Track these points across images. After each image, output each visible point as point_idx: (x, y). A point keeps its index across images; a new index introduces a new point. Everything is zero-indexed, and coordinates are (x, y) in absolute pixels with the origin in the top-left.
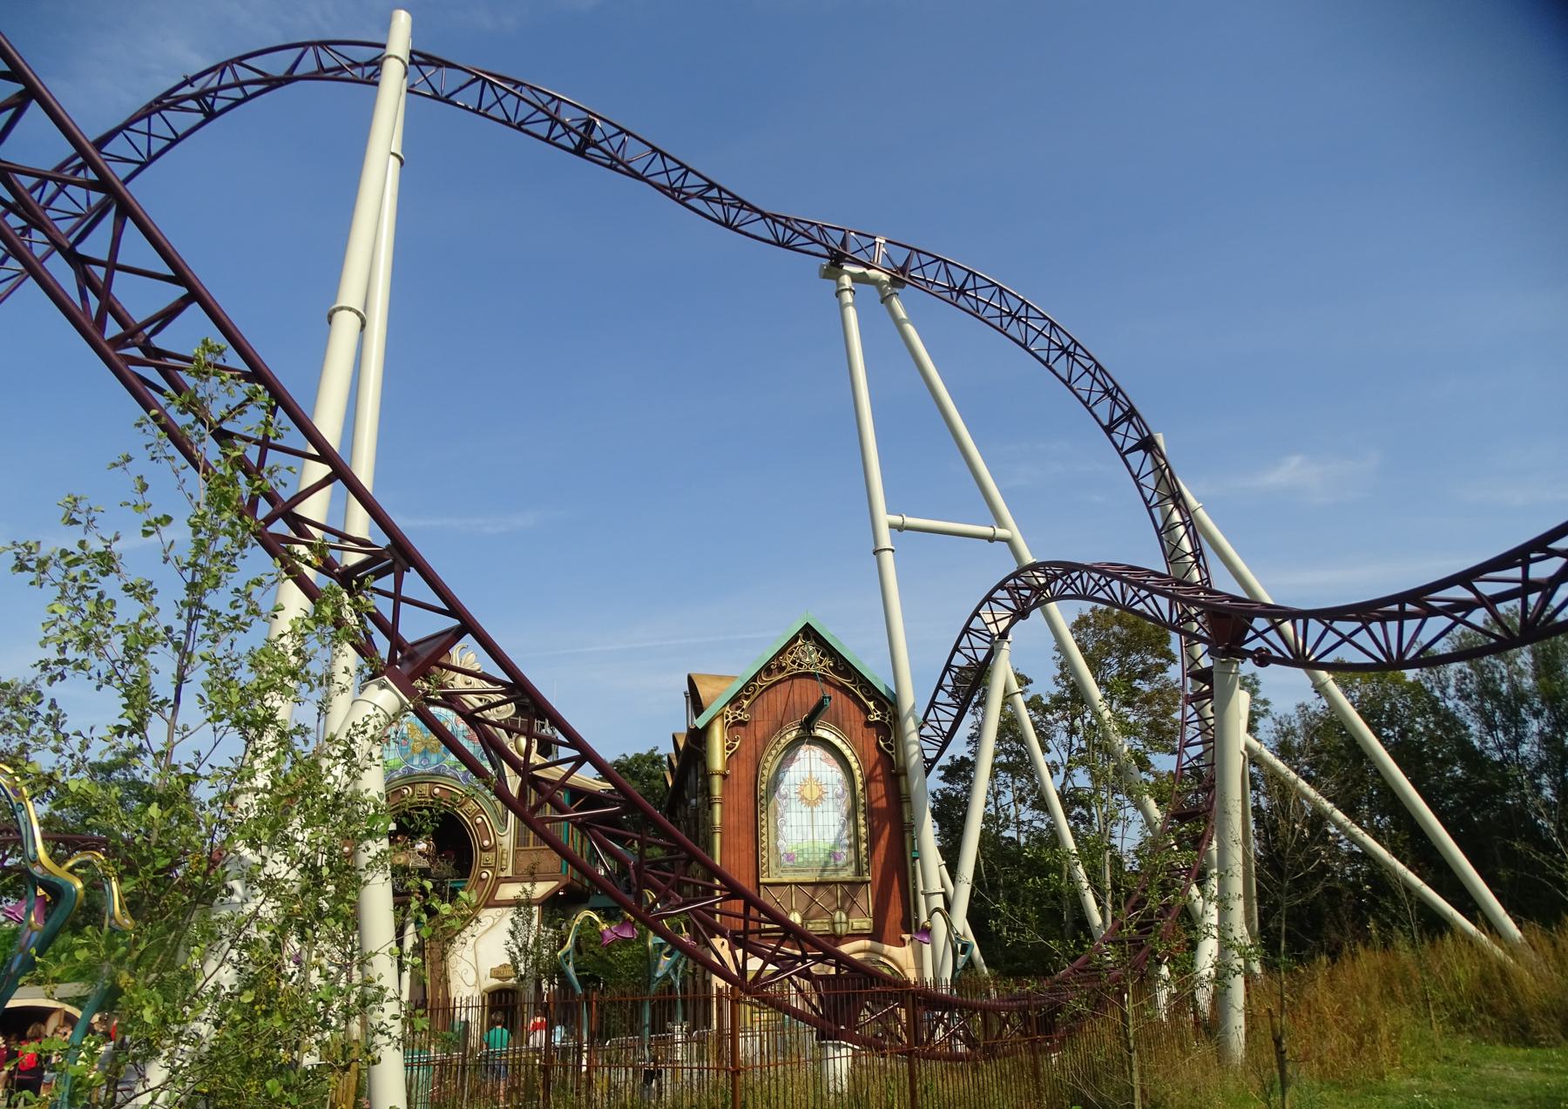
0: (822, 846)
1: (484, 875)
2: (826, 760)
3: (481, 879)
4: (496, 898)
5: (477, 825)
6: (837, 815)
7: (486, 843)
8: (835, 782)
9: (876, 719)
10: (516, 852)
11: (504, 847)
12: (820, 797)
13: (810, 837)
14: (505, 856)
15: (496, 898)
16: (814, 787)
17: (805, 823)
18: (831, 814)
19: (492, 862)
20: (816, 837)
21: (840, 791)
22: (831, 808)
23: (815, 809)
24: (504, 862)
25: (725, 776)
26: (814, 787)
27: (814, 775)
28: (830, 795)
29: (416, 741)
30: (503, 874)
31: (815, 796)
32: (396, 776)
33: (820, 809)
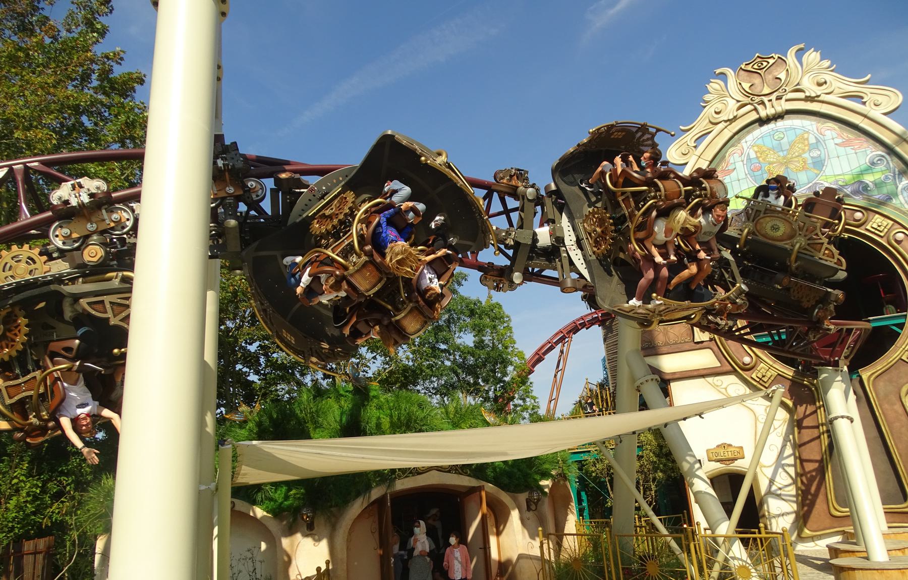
5: (899, 242)
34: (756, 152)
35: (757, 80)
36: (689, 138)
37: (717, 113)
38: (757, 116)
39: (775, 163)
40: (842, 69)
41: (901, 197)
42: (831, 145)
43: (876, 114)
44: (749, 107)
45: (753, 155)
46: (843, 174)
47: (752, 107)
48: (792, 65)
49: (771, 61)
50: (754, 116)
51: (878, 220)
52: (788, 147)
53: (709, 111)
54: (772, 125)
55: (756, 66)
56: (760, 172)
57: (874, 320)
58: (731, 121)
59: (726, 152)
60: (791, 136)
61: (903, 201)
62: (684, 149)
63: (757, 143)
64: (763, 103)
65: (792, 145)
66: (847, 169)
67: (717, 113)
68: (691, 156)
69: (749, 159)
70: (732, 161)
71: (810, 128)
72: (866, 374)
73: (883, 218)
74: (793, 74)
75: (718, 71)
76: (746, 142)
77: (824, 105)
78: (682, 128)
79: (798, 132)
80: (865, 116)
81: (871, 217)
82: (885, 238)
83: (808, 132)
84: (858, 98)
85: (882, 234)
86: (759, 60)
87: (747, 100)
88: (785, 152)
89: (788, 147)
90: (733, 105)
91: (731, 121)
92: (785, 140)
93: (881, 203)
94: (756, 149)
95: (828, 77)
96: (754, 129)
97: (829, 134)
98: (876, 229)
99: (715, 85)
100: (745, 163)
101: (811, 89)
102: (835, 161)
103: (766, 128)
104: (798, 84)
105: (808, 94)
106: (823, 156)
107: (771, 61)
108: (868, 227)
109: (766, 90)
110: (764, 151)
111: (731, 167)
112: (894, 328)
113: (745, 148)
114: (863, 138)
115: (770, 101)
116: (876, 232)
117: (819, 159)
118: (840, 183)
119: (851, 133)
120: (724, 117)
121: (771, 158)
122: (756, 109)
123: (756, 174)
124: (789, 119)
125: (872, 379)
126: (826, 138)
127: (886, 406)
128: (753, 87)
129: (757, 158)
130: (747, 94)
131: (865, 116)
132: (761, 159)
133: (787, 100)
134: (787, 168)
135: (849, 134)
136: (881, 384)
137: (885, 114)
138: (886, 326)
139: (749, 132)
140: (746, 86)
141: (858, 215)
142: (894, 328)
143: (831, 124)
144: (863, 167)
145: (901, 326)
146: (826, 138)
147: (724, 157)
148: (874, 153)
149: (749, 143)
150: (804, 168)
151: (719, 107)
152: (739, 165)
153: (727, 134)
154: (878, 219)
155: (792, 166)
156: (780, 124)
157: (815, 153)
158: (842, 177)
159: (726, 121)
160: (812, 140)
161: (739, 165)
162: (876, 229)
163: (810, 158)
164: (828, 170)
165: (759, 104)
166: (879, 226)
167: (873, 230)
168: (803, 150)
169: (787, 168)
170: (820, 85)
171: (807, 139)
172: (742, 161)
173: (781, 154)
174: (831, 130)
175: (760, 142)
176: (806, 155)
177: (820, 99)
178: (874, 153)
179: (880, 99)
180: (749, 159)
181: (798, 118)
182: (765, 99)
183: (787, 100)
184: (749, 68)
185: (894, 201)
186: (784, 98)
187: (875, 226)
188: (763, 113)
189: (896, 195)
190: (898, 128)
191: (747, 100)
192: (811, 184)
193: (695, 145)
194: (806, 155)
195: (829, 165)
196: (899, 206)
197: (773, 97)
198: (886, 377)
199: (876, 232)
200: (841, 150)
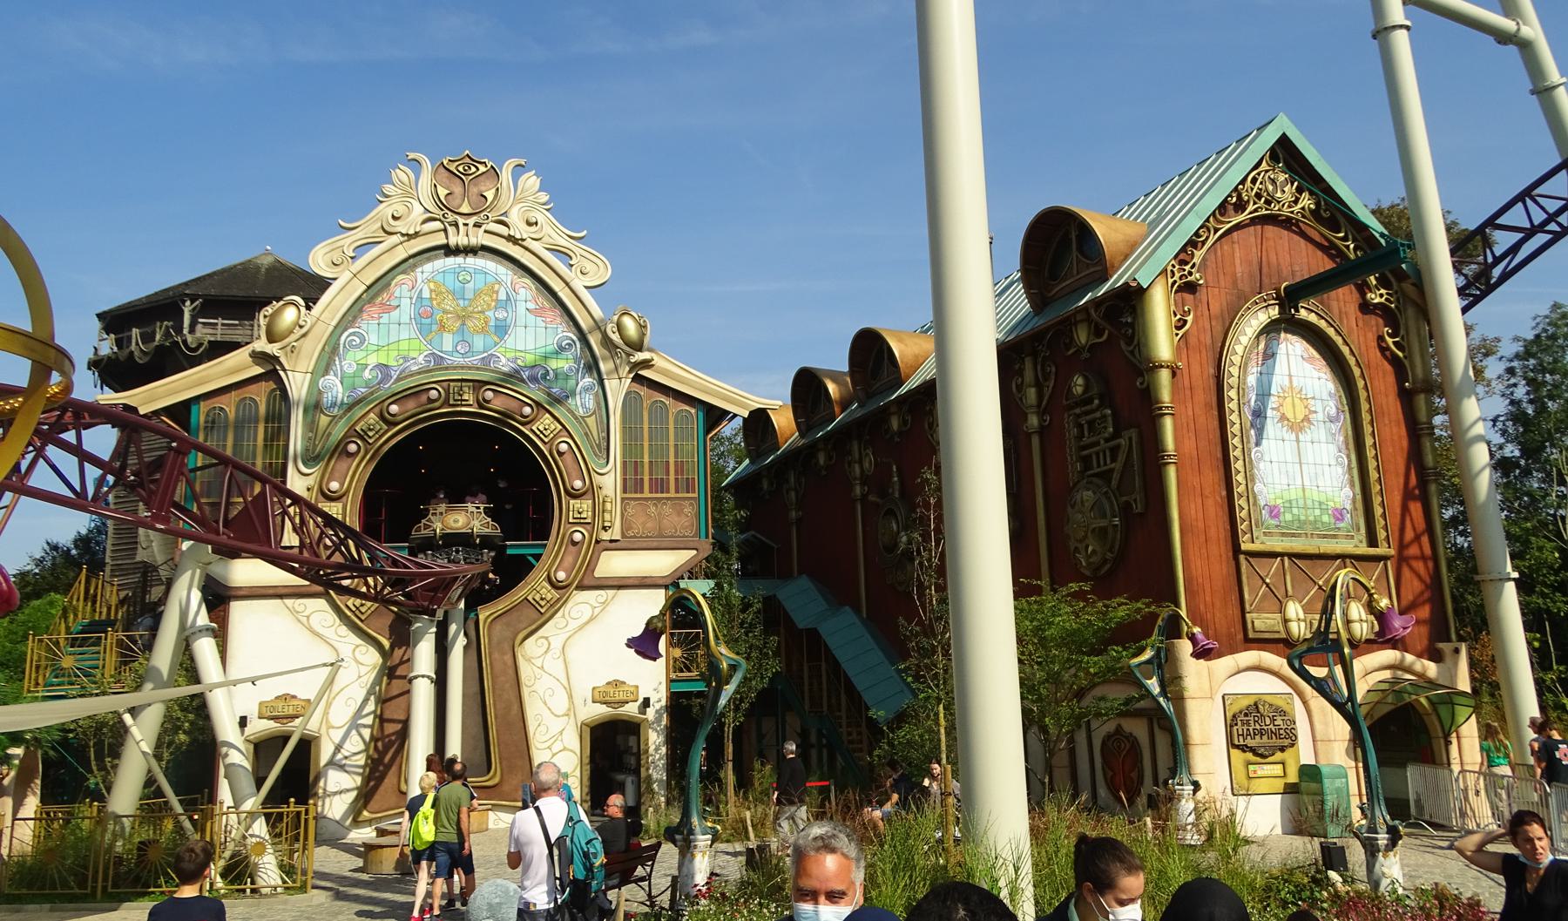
0: (1316, 498)
1: (577, 536)
2: (1310, 360)
3: (574, 543)
4: (597, 574)
5: (561, 454)
6: (1333, 449)
7: (578, 484)
8: (1325, 396)
11: (604, 492)
12: (1306, 419)
13: (1299, 482)
14: (608, 506)
15: (597, 574)
16: (1297, 401)
17: (1289, 459)
18: (1324, 446)
19: (587, 515)
21: (1333, 411)
22: (1323, 438)
23: (1301, 437)
24: (607, 517)
26: (1297, 401)
27: (1295, 384)
28: (1320, 416)
29: (445, 312)
30: (605, 536)
31: (1300, 417)
32: (414, 368)
33: (1309, 438)
34: (431, 291)
35: (458, 189)
36: (348, 242)
37: (394, 218)
38: (445, 241)
39: (451, 313)
40: (559, 211)
41: (578, 397)
42: (521, 308)
43: (579, 284)
44: (437, 225)
45: (426, 294)
46: (525, 352)
47: (442, 227)
48: (504, 184)
49: (482, 169)
50: (440, 240)
51: (547, 421)
52: (471, 296)
53: (385, 210)
54: (459, 260)
55: (461, 169)
56: (428, 321)
57: (511, 545)
58: (410, 237)
59: (392, 280)
60: (479, 282)
61: (579, 404)
62: (336, 257)
63: (436, 278)
64: (456, 225)
65: (478, 294)
66: (531, 346)
67: (394, 218)
68: (343, 271)
69: (420, 297)
70: (397, 294)
71: (504, 278)
72: (484, 614)
73: (552, 419)
74: (503, 197)
75: (412, 155)
76: (422, 273)
77: (527, 253)
79: (490, 279)
80: (567, 284)
81: (540, 416)
82: (548, 445)
83: (499, 283)
85: (546, 440)
86: (468, 160)
87: (438, 213)
88: (466, 302)
89: (471, 296)
90: (418, 212)
91: (410, 237)
92: (471, 285)
93: (557, 401)
94: (432, 285)
95: (541, 217)
96: (436, 257)
97: (522, 291)
98: (541, 432)
99: (402, 174)
100: (414, 302)
101: (520, 230)
102: (520, 330)
104: (505, 214)
105: (512, 233)
106: (508, 320)
107: (482, 169)
108: (534, 428)
109: (465, 209)
110: (441, 293)
111: (394, 303)
112: (530, 558)
113: (419, 281)
114: (558, 311)
115: (466, 225)
116: (541, 436)
117: (503, 324)
118: (519, 362)
119: (548, 300)
120: (401, 227)
121: (449, 304)
122: (445, 230)
123: (424, 321)
124: (483, 257)
125: (489, 620)
127: (496, 655)
128: (450, 197)
129: (431, 299)
130: (440, 204)
131: (567, 284)
132: (435, 302)
133: (486, 231)
135: (544, 302)
136: (498, 627)
137: (586, 287)
138: (523, 556)
139: (429, 260)
140: (442, 192)
141: (527, 410)
142: (530, 558)
143: (528, 281)
144: (550, 349)
145: (538, 557)
146: (519, 297)
147: (389, 284)
148: (565, 334)
149: (425, 275)
150: (483, 331)
151: (400, 209)
152: (405, 303)
153: (401, 254)
154: (547, 419)
155: (470, 324)
156: (470, 260)
157: (501, 314)
158: (523, 354)
159: (403, 235)
160: (503, 296)
161: (405, 303)
162: (541, 432)
163: (493, 318)
164: (510, 341)
165: (450, 225)
166: (545, 429)
167: (538, 433)
168: (489, 305)
170: (529, 224)
171: (497, 292)
172: (411, 298)
173: (461, 302)
174: (526, 291)
175: (439, 278)
176: (490, 314)
177: (524, 243)
178: (565, 334)
179: (589, 267)
180: (420, 297)
181: (493, 260)
182: (461, 221)
183: (486, 231)
184: (452, 168)
185: (570, 401)
186: (484, 227)
187: (541, 428)
188: (453, 241)
189: (573, 393)
190: (598, 312)
191: (438, 213)
192: (486, 354)
193: (353, 255)
194: (490, 314)
195: (513, 335)
196: (573, 408)
197: (471, 221)
198: (504, 619)
199: (541, 436)
200: (531, 318)
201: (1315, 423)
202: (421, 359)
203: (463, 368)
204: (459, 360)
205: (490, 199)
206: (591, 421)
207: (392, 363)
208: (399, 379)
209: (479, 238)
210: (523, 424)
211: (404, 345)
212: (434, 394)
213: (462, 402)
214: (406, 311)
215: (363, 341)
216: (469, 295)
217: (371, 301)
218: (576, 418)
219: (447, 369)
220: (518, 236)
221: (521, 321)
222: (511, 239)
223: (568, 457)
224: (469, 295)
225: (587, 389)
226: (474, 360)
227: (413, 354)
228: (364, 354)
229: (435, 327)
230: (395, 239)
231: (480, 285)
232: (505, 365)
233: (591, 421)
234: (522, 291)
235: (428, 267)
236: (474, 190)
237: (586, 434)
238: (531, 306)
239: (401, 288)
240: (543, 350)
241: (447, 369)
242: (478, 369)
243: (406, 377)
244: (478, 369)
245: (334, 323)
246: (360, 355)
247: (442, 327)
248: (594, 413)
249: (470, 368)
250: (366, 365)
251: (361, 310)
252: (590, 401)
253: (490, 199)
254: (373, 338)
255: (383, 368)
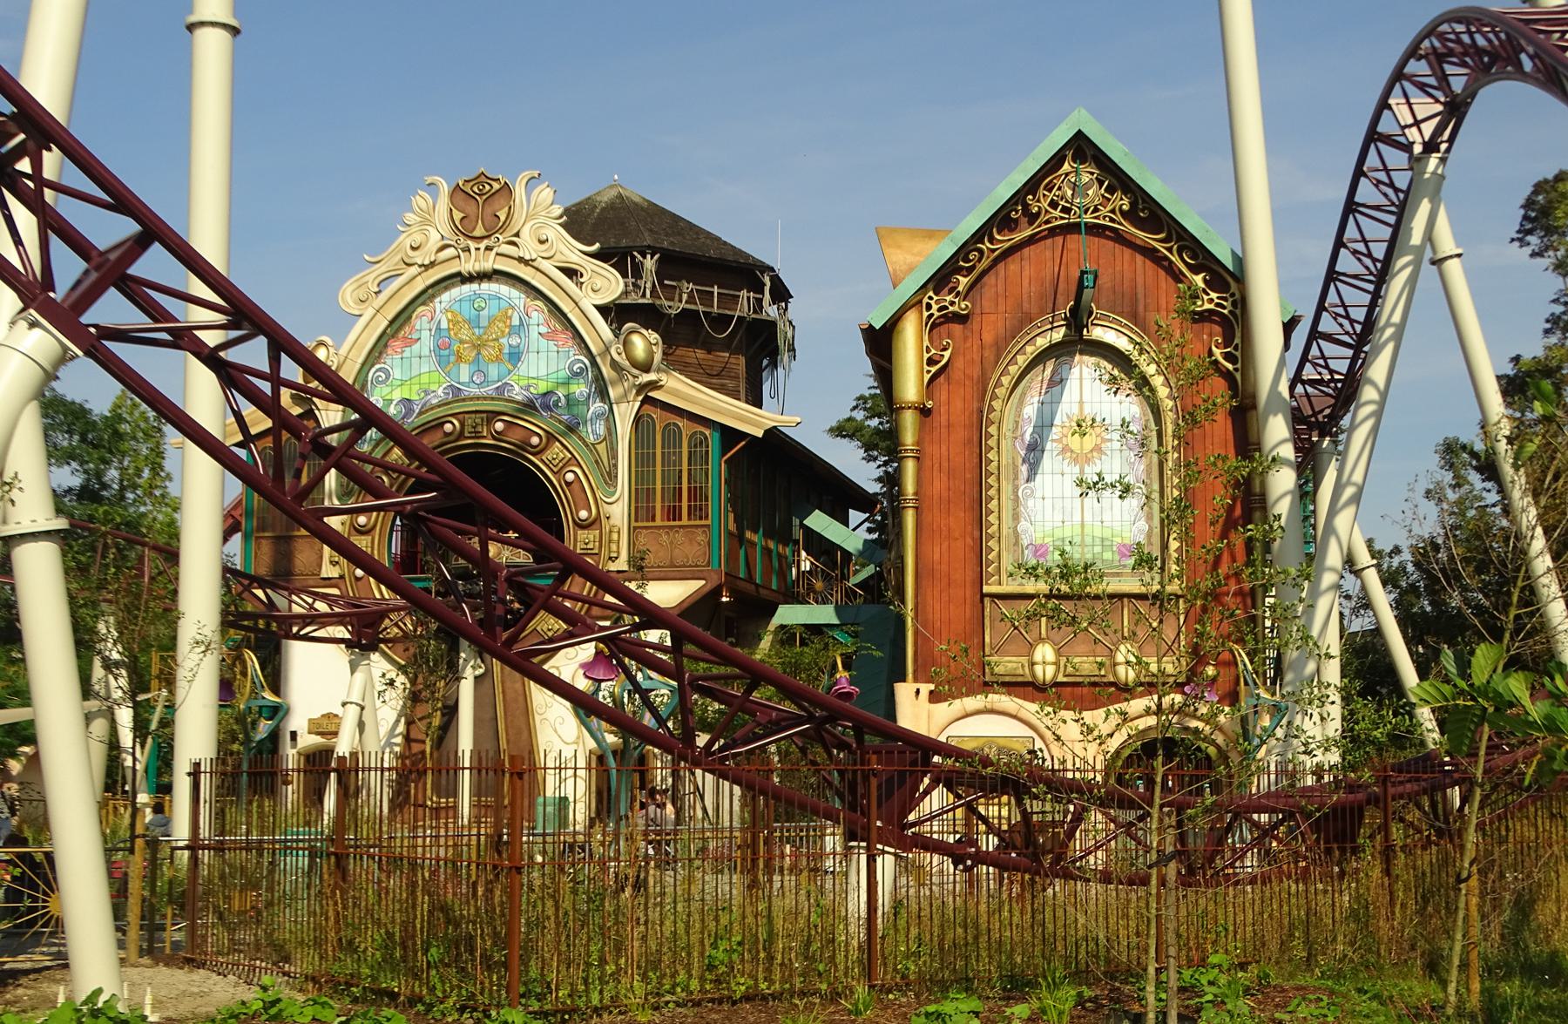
7: (583, 514)
9: (1207, 306)
10: (632, 531)
11: (612, 521)
13: (1077, 517)
20: (1088, 517)
25: (924, 412)
29: (462, 342)
32: (435, 401)
34: (449, 321)
36: (372, 276)
37: (413, 248)
42: (534, 334)
45: (444, 325)
46: (537, 378)
52: (486, 324)
53: (405, 241)
54: (475, 286)
55: (476, 189)
58: (427, 267)
60: (492, 309)
62: (362, 294)
65: (492, 320)
67: (413, 248)
69: (439, 328)
70: (417, 327)
71: (517, 302)
74: (516, 216)
75: (429, 180)
78: (367, 258)
84: (571, 273)
89: (486, 324)
90: (434, 239)
91: (427, 267)
96: (453, 285)
97: (535, 314)
99: (421, 200)
102: (533, 356)
103: (467, 288)
109: (479, 231)
110: (458, 322)
111: (415, 336)
115: (478, 249)
120: (419, 258)
124: (497, 281)
126: (531, 321)
128: (465, 221)
129: (449, 329)
130: (457, 230)
133: (497, 254)
134: (479, 353)
139: (447, 288)
140: (458, 215)
146: (531, 321)
147: (410, 317)
149: (443, 305)
150: (498, 359)
151: (417, 238)
152: (425, 334)
153: (419, 285)
155: (484, 352)
156: (485, 286)
157: (514, 341)
159: (420, 266)
160: (516, 322)
161: (425, 334)
164: (523, 368)
168: (503, 332)
169: (479, 353)
170: (542, 242)
171: (510, 318)
173: (476, 331)
174: (538, 316)
175: (456, 307)
176: (503, 341)
177: (534, 264)
179: (599, 283)
180: (439, 328)
182: (472, 245)
188: (469, 265)
194: (503, 341)
196: (584, 435)
197: (482, 245)
200: (543, 342)
201: (1109, 453)
202: (440, 392)
203: (478, 399)
204: (475, 391)
205: (503, 218)
206: (602, 448)
207: (414, 397)
208: (421, 413)
209: (489, 262)
210: (533, 454)
211: (425, 379)
212: (448, 427)
213: (477, 435)
214: (426, 343)
215: (388, 376)
216: (484, 323)
217: (393, 336)
218: (587, 446)
219: (464, 400)
220: (527, 257)
221: (533, 347)
222: (521, 260)
223: (575, 486)
224: (484, 323)
225: (598, 416)
226: (489, 390)
227: (433, 387)
228: (389, 389)
229: (452, 359)
230: (414, 270)
231: (494, 311)
232: (518, 394)
233: (602, 448)
234: (535, 314)
235: (446, 296)
236: (489, 210)
237: (597, 462)
238: (544, 330)
239: (421, 321)
240: (555, 376)
241: (464, 400)
242: (493, 399)
243: (427, 411)
244: (493, 399)
245: (360, 360)
246: (386, 390)
247: (459, 358)
248: (605, 439)
249: (485, 398)
250: (392, 400)
251: (386, 346)
252: (601, 428)
253: (503, 218)
254: (397, 374)
255: (406, 402)
